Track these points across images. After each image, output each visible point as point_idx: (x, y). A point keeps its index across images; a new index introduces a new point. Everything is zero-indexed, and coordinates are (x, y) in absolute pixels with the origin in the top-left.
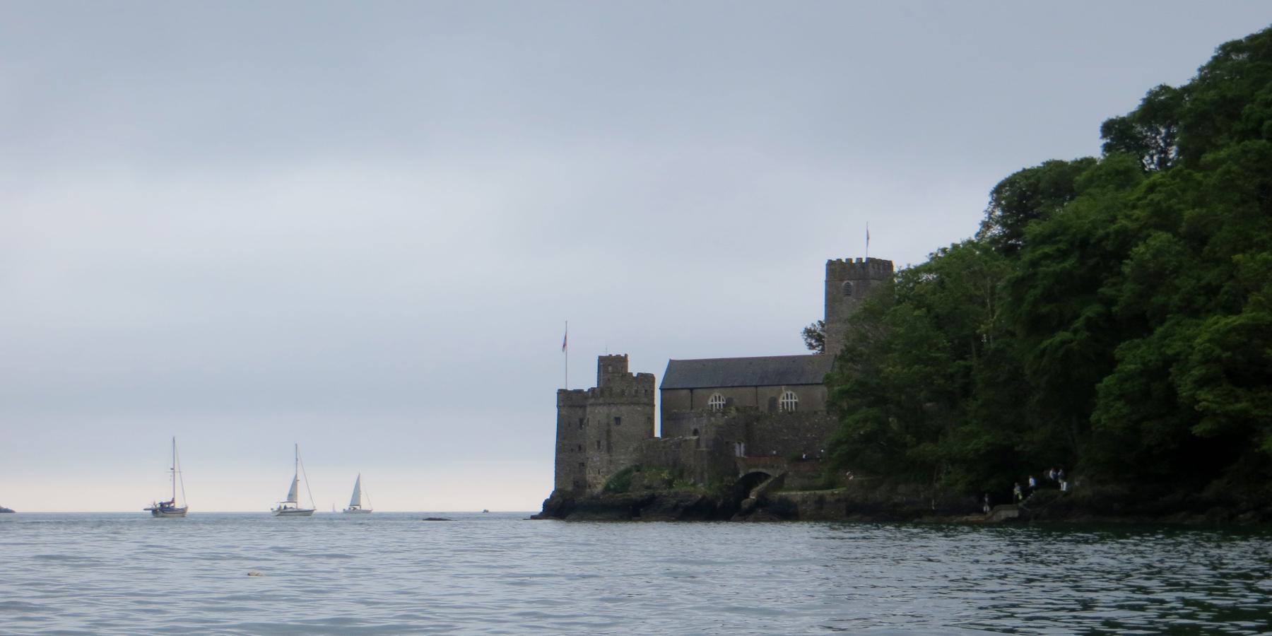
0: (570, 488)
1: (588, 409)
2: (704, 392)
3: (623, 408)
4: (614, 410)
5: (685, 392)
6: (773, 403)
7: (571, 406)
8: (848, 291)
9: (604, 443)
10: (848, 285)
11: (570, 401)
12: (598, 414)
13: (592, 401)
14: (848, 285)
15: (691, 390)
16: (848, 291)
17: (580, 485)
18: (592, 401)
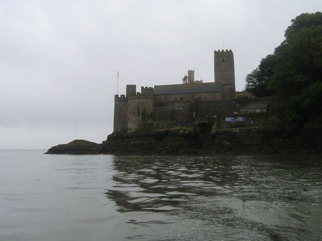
0: (120, 131)
1: (129, 102)
2: (171, 96)
3: (144, 100)
4: (141, 100)
5: (163, 96)
6: (200, 98)
7: (121, 101)
8: (223, 61)
9: (136, 113)
10: (223, 59)
11: (119, 100)
12: (132, 103)
13: (132, 97)
14: (223, 59)
15: (166, 95)
16: (223, 61)
17: (125, 131)
18: (132, 97)
